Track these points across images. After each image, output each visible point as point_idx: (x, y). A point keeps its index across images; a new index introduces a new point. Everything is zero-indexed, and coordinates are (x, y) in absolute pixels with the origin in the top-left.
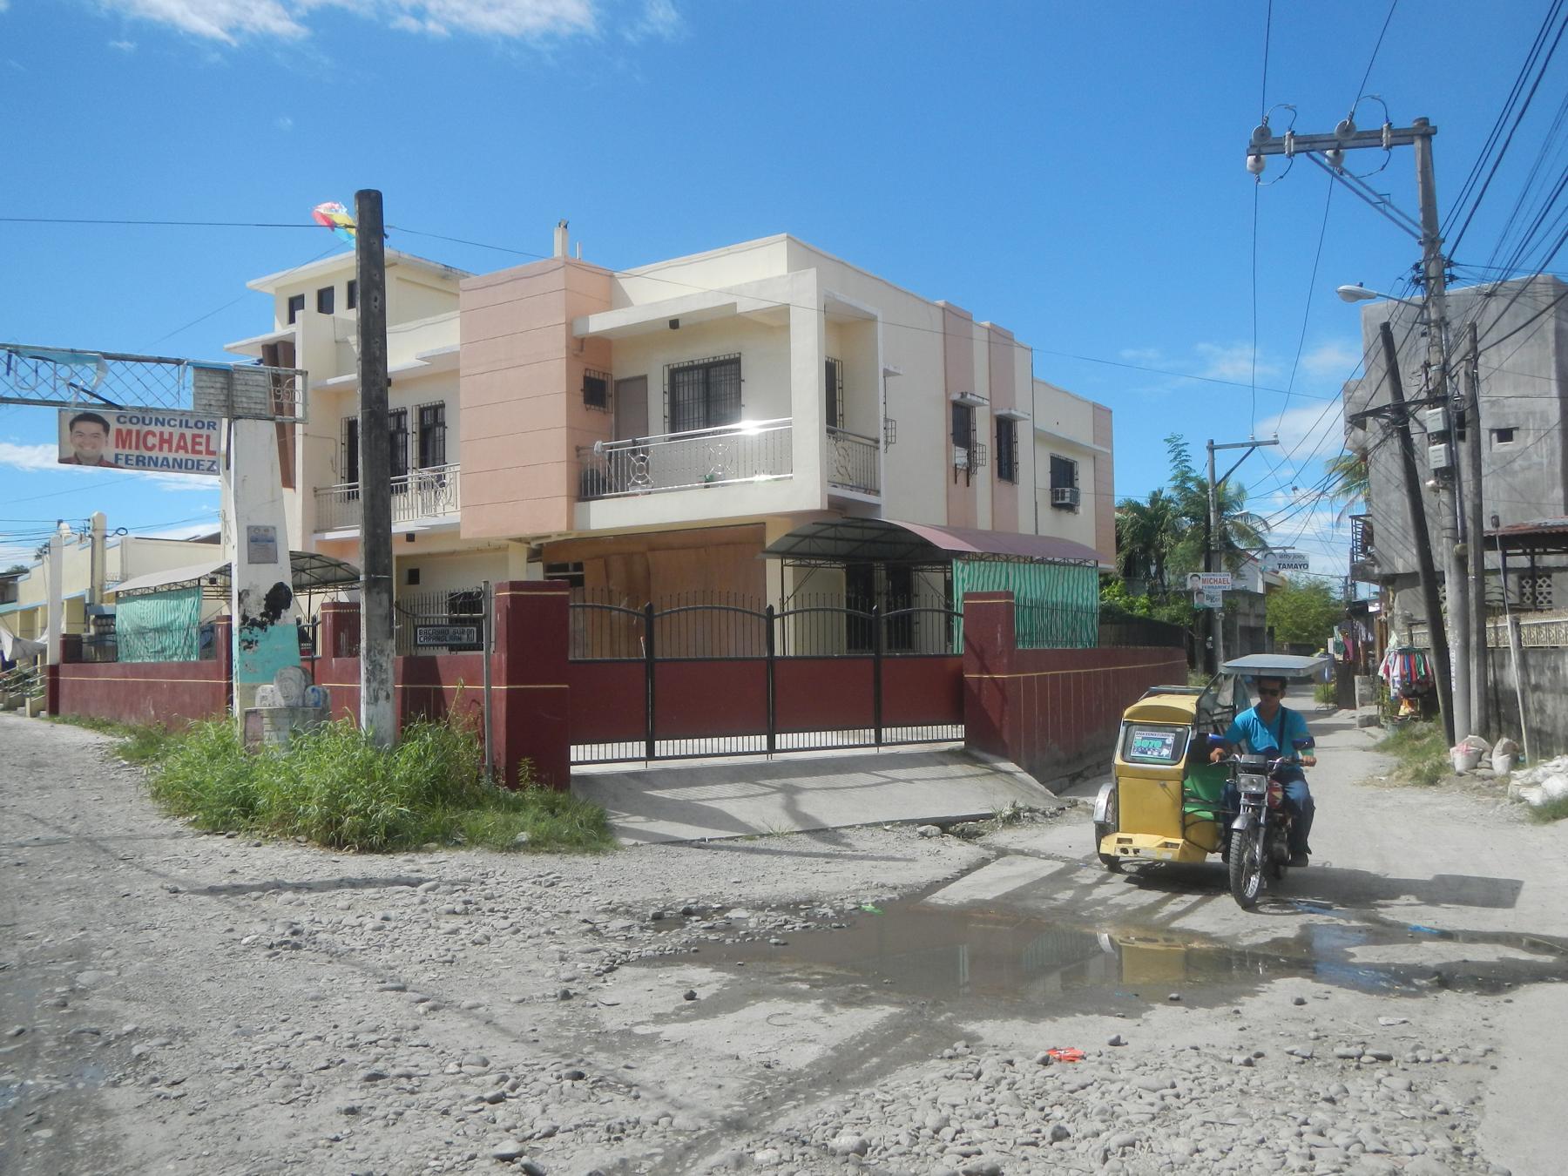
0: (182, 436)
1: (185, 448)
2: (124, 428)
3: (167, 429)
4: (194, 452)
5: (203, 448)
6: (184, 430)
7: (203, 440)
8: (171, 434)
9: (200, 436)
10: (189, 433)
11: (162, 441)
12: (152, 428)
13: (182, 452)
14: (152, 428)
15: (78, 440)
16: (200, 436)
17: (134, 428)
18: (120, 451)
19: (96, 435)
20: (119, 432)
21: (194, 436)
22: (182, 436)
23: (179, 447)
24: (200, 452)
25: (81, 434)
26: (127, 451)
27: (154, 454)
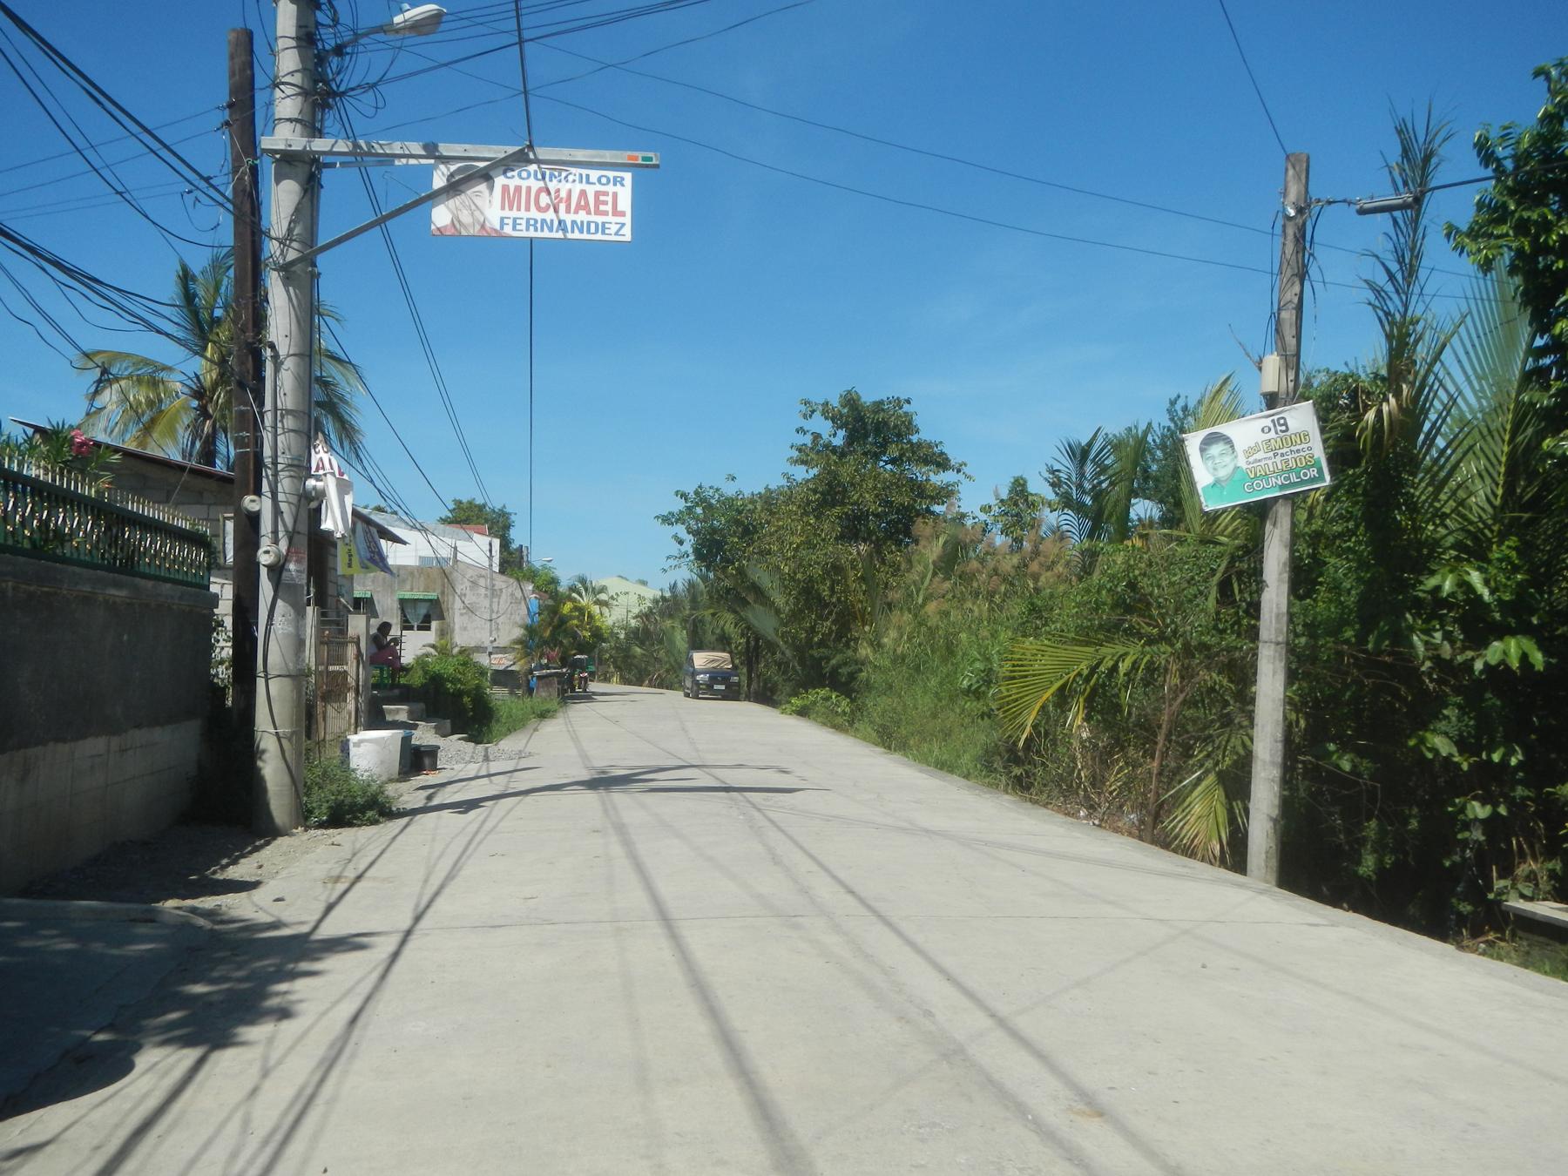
0: (583, 193)
1: (586, 208)
4: (598, 212)
5: (609, 208)
6: (584, 186)
7: (609, 199)
8: (569, 192)
9: (606, 194)
10: (591, 191)
13: (582, 213)
16: (606, 194)
17: (524, 184)
18: (507, 213)
21: (597, 194)
22: (583, 193)
24: (605, 213)
26: (514, 213)
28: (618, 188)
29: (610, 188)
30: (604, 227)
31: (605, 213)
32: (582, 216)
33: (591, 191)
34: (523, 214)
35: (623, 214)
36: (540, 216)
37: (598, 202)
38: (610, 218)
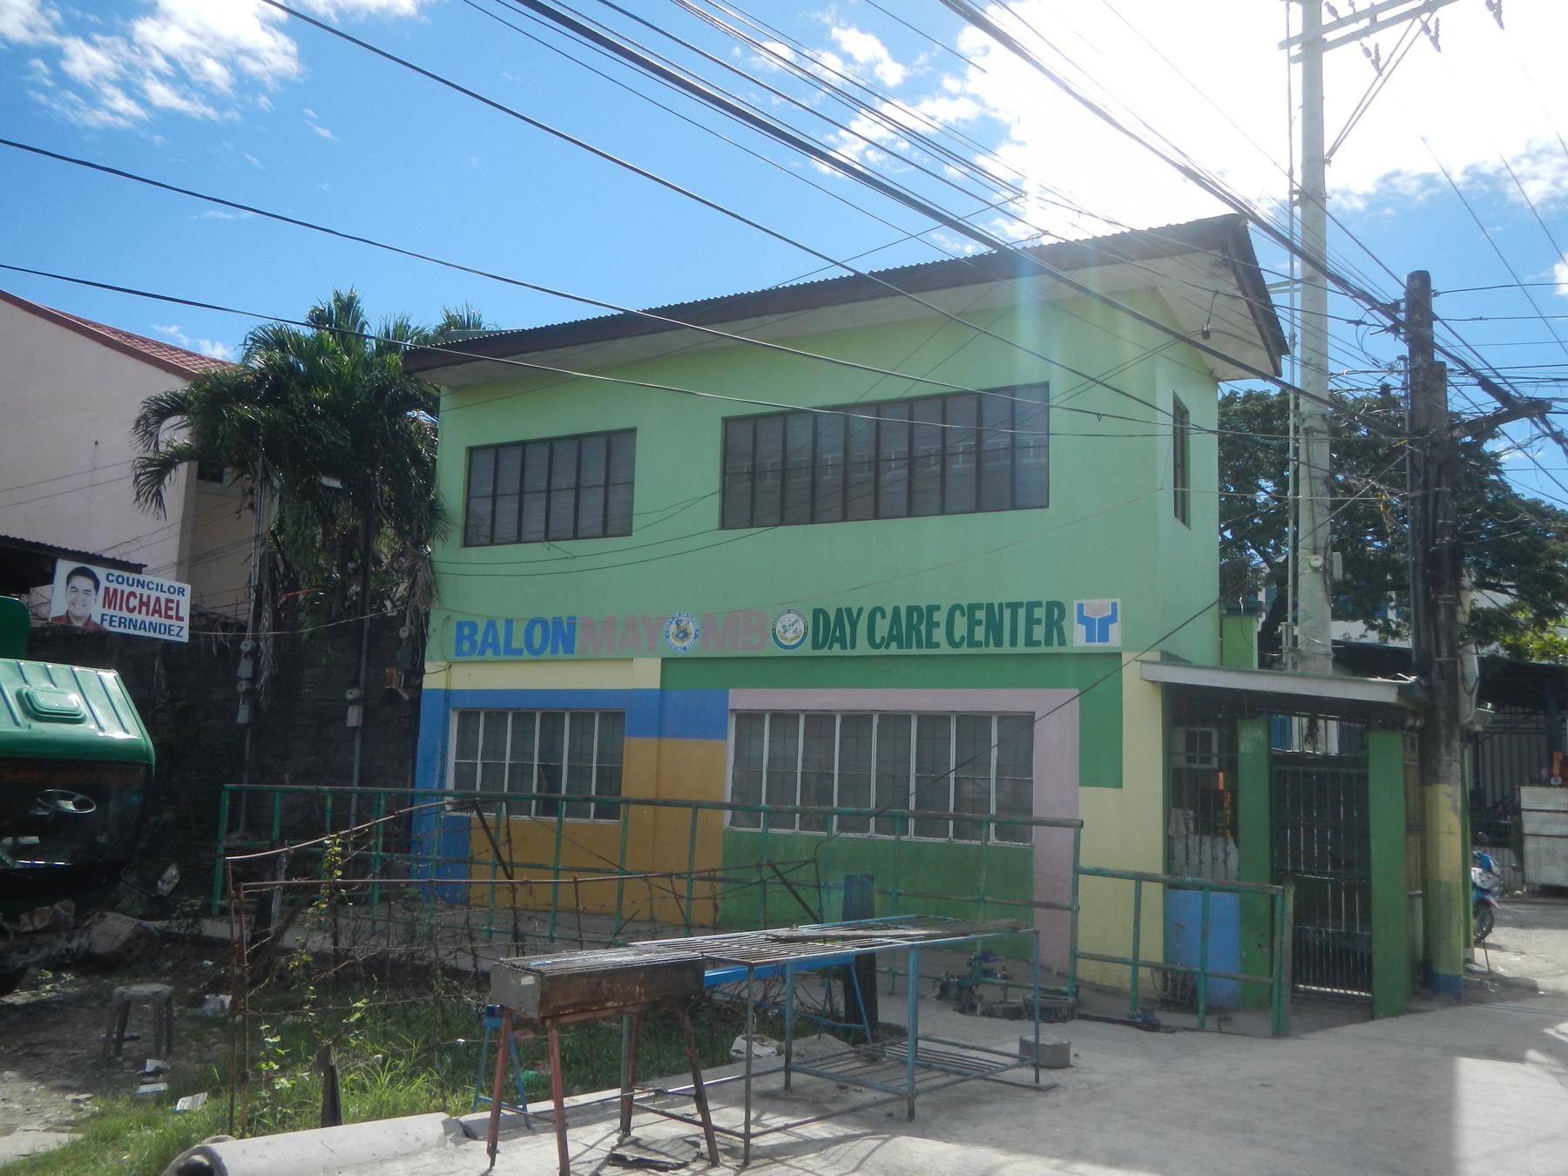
0: (158, 600)
1: (159, 612)
2: (112, 586)
3: (146, 592)
6: (159, 594)
10: (163, 597)
11: (142, 604)
12: (133, 589)
14: (133, 589)
15: (73, 596)
17: (120, 587)
18: (106, 611)
19: (87, 592)
20: (107, 589)
21: (168, 601)
22: (158, 600)
23: (155, 611)
25: (75, 590)
26: (111, 612)
27: (135, 616)
28: (180, 598)
29: (175, 597)
30: (169, 629)
31: (170, 617)
32: (156, 619)
33: (163, 597)
34: (117, 613)
35: (181, 619)
36: (128, 615)
37: (167, 608)
38: (173, 622)
